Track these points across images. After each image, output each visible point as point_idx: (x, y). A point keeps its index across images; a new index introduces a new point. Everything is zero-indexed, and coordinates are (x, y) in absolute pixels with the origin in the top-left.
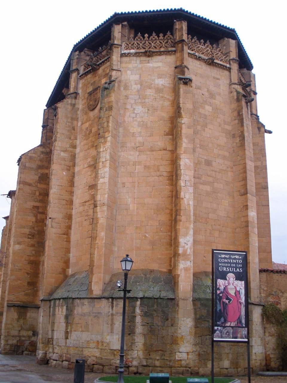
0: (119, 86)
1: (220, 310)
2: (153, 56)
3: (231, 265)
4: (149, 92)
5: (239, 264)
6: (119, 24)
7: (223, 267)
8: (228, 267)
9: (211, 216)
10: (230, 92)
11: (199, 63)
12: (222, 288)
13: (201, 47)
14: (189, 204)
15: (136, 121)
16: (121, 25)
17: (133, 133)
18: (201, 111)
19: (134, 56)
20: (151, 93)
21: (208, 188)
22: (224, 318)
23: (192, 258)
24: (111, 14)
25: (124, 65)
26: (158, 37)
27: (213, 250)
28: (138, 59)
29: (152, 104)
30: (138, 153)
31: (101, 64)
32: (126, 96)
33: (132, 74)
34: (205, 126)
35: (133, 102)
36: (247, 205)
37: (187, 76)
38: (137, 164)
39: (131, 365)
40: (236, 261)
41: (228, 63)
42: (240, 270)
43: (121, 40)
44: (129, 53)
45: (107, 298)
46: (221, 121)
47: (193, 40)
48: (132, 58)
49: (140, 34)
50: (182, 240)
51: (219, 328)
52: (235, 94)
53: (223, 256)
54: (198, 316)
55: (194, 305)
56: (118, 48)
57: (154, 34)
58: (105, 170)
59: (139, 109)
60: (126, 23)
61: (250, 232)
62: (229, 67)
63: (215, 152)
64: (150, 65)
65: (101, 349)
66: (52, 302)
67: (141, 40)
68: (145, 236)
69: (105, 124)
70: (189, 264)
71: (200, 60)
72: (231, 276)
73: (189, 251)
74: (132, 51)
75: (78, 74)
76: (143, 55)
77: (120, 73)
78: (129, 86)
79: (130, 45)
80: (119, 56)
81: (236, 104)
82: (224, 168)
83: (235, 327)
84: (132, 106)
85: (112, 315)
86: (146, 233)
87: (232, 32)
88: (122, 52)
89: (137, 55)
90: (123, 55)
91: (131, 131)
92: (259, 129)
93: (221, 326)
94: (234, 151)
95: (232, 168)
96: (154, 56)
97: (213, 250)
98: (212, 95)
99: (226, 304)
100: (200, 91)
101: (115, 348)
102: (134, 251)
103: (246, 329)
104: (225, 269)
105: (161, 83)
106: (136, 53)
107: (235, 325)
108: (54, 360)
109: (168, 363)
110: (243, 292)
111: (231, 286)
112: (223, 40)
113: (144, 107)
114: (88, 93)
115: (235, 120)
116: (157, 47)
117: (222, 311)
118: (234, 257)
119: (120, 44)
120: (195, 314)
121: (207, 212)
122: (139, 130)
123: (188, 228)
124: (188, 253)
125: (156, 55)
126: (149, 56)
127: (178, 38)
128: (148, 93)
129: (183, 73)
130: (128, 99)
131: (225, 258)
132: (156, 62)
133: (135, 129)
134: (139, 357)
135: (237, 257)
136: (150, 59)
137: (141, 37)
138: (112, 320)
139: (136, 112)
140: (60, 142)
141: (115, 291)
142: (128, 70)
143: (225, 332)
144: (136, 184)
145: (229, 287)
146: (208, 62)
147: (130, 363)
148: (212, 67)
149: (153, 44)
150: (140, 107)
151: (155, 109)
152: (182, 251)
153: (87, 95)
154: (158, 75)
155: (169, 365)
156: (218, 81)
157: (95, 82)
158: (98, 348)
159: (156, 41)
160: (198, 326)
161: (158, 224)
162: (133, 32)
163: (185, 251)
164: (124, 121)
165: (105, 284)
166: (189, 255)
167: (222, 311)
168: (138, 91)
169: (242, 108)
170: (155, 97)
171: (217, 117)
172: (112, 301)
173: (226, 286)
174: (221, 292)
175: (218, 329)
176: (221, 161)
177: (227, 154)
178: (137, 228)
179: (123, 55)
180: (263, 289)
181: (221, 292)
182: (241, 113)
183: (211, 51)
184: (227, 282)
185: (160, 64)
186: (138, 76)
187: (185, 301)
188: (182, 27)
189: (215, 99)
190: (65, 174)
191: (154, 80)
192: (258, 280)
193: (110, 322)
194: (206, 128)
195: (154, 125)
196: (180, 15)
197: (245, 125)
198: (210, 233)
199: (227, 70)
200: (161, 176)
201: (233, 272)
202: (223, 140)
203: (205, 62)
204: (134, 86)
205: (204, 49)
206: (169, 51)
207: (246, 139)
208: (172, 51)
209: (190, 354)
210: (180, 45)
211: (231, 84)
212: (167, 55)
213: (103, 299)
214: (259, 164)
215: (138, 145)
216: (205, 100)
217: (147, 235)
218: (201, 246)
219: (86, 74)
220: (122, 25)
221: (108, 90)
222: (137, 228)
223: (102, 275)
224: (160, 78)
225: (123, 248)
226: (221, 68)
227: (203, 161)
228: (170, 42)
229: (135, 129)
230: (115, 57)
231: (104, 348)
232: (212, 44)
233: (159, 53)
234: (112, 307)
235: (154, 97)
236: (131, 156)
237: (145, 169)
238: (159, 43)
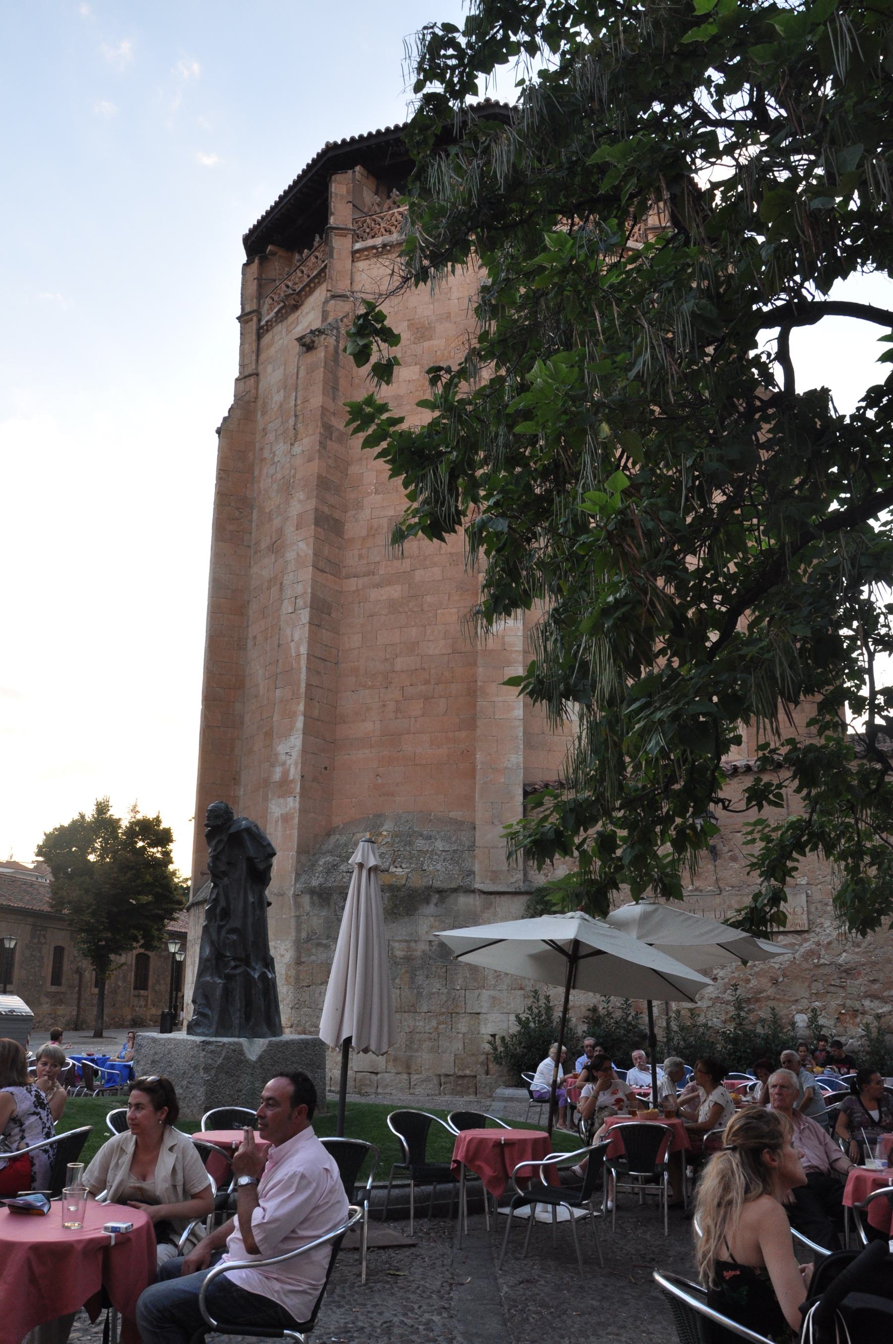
9: (400, 663)
14: (299, 655)
21: (395, 591)
23: (298, 790)
50: (281, 749)
54: (304, 935)
55: (298, 905)
61: (479, 684)
70: (292, 804)
120: (298, 930)
123: (292, 715)
124: (291, 777)
163: (285, 773)
166: (292, 781)
189: (430, 338)
198: (397, 710)
218: (367, 751)
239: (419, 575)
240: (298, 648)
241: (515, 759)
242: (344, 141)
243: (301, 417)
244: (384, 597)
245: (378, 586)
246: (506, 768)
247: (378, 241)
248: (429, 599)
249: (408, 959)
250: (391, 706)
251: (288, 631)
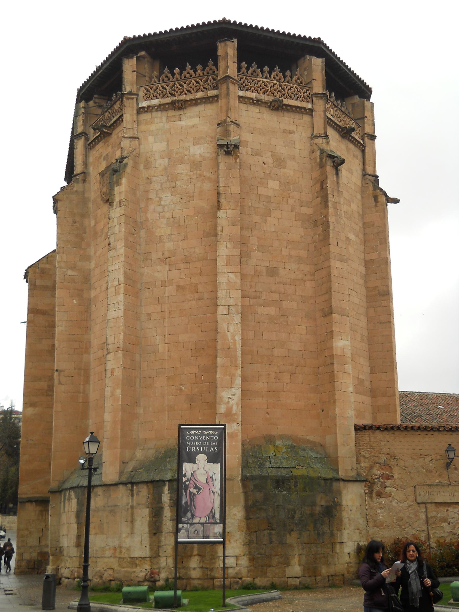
0: (136, 167)
1: (186, 503)
2: (185, 108)
3: (202, 443)
4: (182, 169)
5: (214, 441)
6: (132, 57)
7: (191, 446)
8: (198, 446)
9: (277, 352)
10: (311, 152)
11: (257, 110)
12: (189, 474)
13: (263, 82)
14: (234, 341)
15: (164, 217)
16: (135, 59)
17: (160, 236)
18: (261, 191)
19: (157, 110)
20: (184, 170)
21: (272, 311)
22: (191, 512)
23: (240, 419)
24: (120, 40)
25: (143, 127)
26: (195, 71)
27: (180, 425)
28: (164, 113)
29: (186, 188)
30: (167, 267)
31: (112, 125)
32: (148, 179)
33: (155, 142)
34: (268, 213)
35: (157, 187)
36: (332, 332)
37: (234, 138)
38: (167, 284)
39: (158, 579)
40: (211, 438)
41: (310, 100)
42: (214, 450)
43: (137, 85)
44: (149, 107)
45: (125, 484)
46: (295, 201)
47: (251, 70)
48: (154, 114)
49: (168, 68)
50: (224, 394)
51: (185, 525)
52: (318, 153)
53: (193, 432)
54: (250, 502)
56: (132, 99)
57: (189, 67)
58: (119, 298)
59: (168, 198)
60: (143, 53)
61: (335, 372)
62: (309, 109)
63: (283, 253)
64: (182, 123)
65: (120, 558)
66: (63, 493)
67: (169, 79)
68: (181, 389)
69: (117, 227)
71: (259, 105)
72: (201, 458)
73: (234, 409)
74: (155, 102)
75: (87, 139)
76: (171, 107)
77: (136, 141)
78: (152, 162)
79: (152, 91)
80: (135, 112)
81: (319, 171)
82: (300, 277)
83: (206, 523)
84: (157, 195)
85: (132, 507)
86: (181, 385)
87: (316, 45)
88: (140, 106)
89: (161, 108)
90: (140, 111)
91: (157, 234)
92: (376, 198)
93: (187, 524)
94: (315, 247)
95: (313, 274)
96: (188, 107)
97: (180, 425)
98: (280, 162)
99: (194, 494)
100: (259, 158)
101: (136, 555)
102: (166, 412)
103: (222, 525)
104: (193, 449)
105: (199, 152)
106: (160, 105)
107: (206, 521)
108: (66, 578)
109: (209, 573)
110: (217, 477)
111: (201, 471)
113: (174, 194)
114: (100, 174)
115: (317, 198)
116: (191, 90)
117: (189, 504)
118: (207, 433)
119: (135, 92)
120: (246, 500)
121: (270, 347)
122: (169, 231)
123: (232, 376)
124: (234, 412)
125: (190, 105)
126: (180, 109)
127: (221, 72)
128: (179, 171)
129: (227, 133)
130: (151, 183)
131: (195, 435)
132: (191, 117)
133: (162, 231)
134: (169, 566)
135: (212, 432)
136: (181, 112)
137: (170, 75)
138: (132, 514)
139: (163, 203)
140: (64, 255)
141: (136, 473)
142: (150, 135)
143: (193, 530)
144: (167, 314)
145: (198, 472)
146: (273, 107)
147: (157, 576)
148: (280, 113)
149: (185, 86)
150: (169, 195)
151: (190, 197)
152: (225, 409)
153: (99, 177)
154: (194, 139)
155: (210, 575)
156: (291, 135)
157: (107, 155)
158: (115, 557)
159: (189, 81)
160: (251, 517)
161: (197, 371)
162: (157, 65)
163: (229, 410)
164: (147, 220)
165: (123, 463)
166: (235, 414)
167: (189, 504)
168: (165, 168)
169: (327, 178)
170: (189, 176)
171: (289, 197)
172: (132, 487)
173: (194, 472)
174: (188, 479)
175: (183, 527)
176: (294, 266)
177: (303, 253)
178: (169, 378)
179: (140, 111)
180: (364, 457)
181: (188, 479)
182: (324, 186)
183: (280, 85)
184: (195, 465)
185: (196, 121)
186: (164, 144)
187: (231, 482)
188: (228, 50)
189: (285, 168)
190: (76, 302)
191: (187, 149)
192: (353, 443)
193: (129, 519)
194: (269, 218)
195: (190, 223)
196: (224, 30)
197: (330, 204)
198: (276, 378)
199: (307, 114)
200: (200, 299)
201: (204, 453)
202: (297, 232)
203: (269, 107)
204: (159, 161)
205: (269, 81)
206: (208, 98)
207: (331, 227)
208: (213, 97)
209: (240, 558)
210: (224, 86)
211: (313, 137)
212: (207, 103)
213: (121, 486)
214: (374, 256)
215: (167, 255)
216: (267, 171)
217: (183, 388)
219: (97, 140)
220: (138, 59)
221: (118, 173)
222: (169, 378)
223: (119, 451)
224: (198, 144)
225: (151, 408)
226: (297, 112)
227: (264, 269)
228: (211, 79)
229: (162, 230)
230: (129, 116)
231: (122, 556)
232: (283, 71)
233: (194, 102)
234: (132, 495)
235: (189, 177)
236: (157, 272)
237: (177, 290)
238: (195, 83)
239: (285, 304)
240: (233, 336)
241: (351, 413)
242: (235, 22)
243: (223, 196)
244: (266, 313)
245: (262, 305)
246: (348, 417)
247: (253, 95)
248: (290, 318)
249: (312, 515)
250: (273, 375)
251: (225, 326)
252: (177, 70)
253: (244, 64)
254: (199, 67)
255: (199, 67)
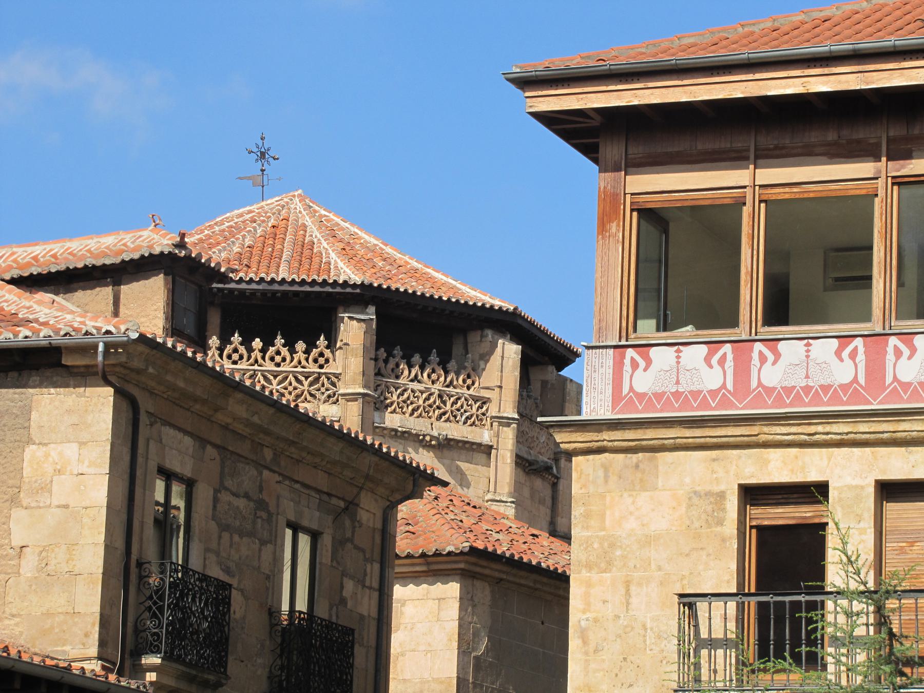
13: (413, 391)
26: (292, 351)
57: (279, 341)
112: (482, 336)
252: (257, 343)
253: (382, 353)
254: (300, 346)
255: (300, 346)
